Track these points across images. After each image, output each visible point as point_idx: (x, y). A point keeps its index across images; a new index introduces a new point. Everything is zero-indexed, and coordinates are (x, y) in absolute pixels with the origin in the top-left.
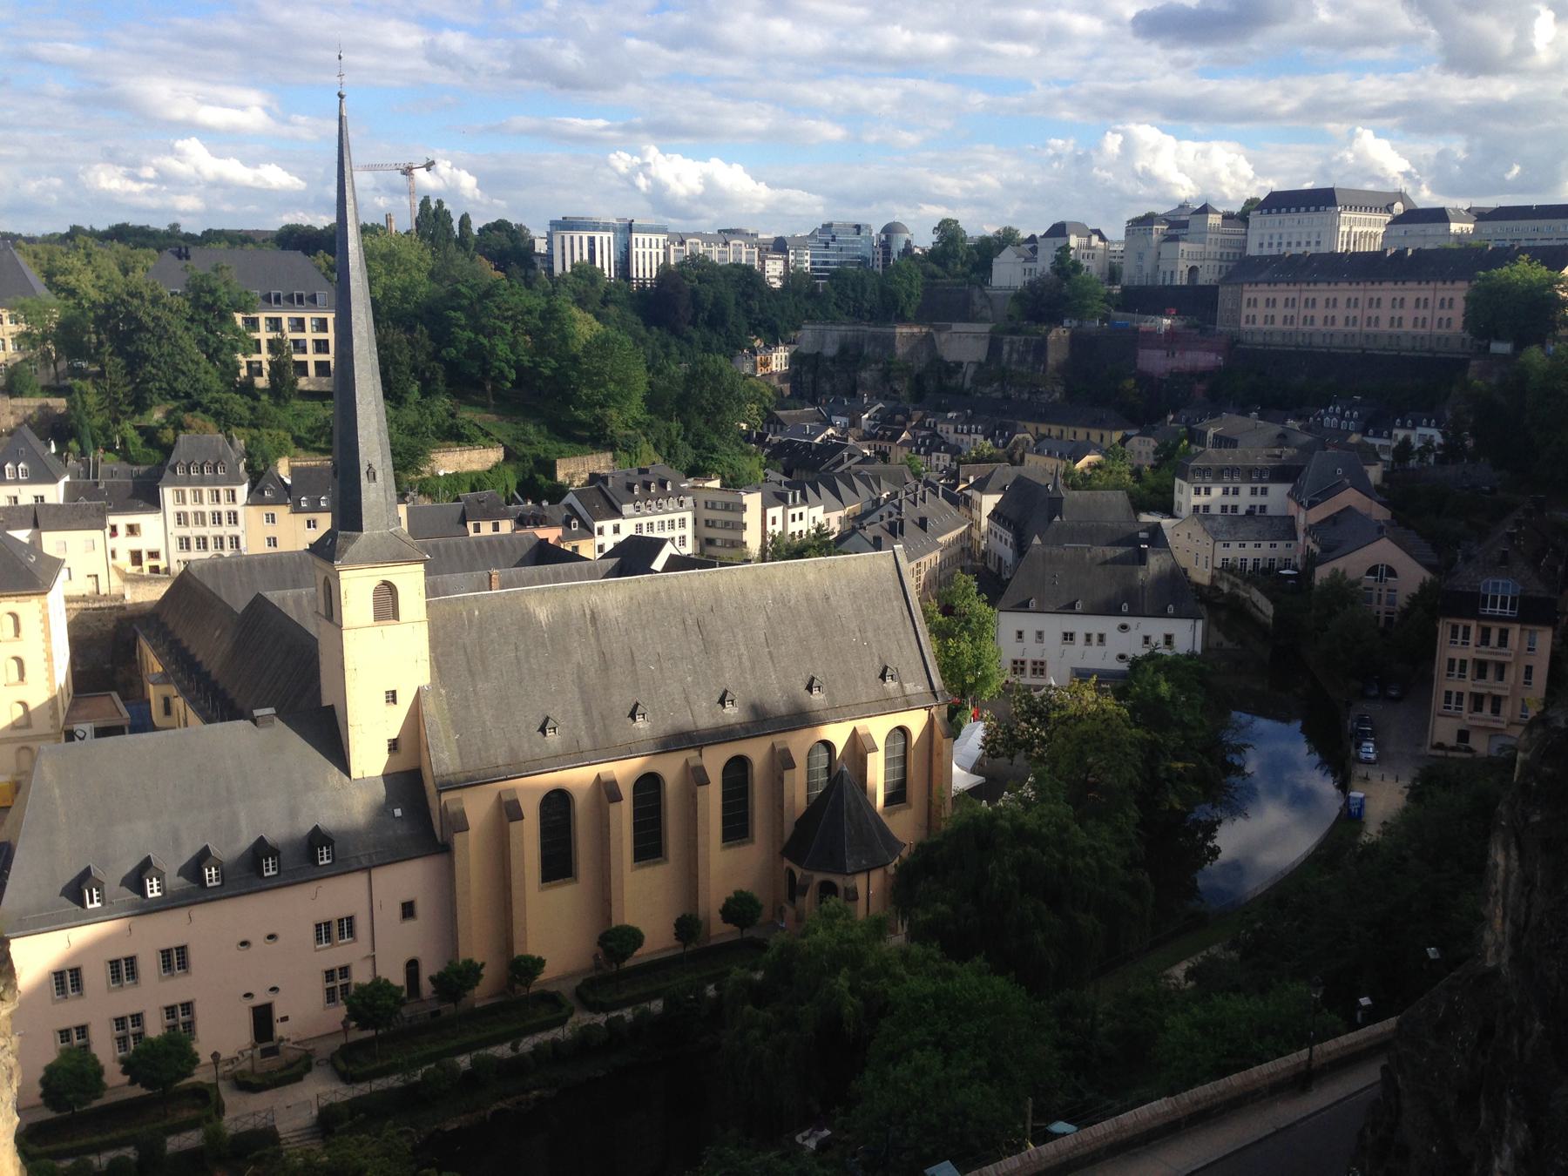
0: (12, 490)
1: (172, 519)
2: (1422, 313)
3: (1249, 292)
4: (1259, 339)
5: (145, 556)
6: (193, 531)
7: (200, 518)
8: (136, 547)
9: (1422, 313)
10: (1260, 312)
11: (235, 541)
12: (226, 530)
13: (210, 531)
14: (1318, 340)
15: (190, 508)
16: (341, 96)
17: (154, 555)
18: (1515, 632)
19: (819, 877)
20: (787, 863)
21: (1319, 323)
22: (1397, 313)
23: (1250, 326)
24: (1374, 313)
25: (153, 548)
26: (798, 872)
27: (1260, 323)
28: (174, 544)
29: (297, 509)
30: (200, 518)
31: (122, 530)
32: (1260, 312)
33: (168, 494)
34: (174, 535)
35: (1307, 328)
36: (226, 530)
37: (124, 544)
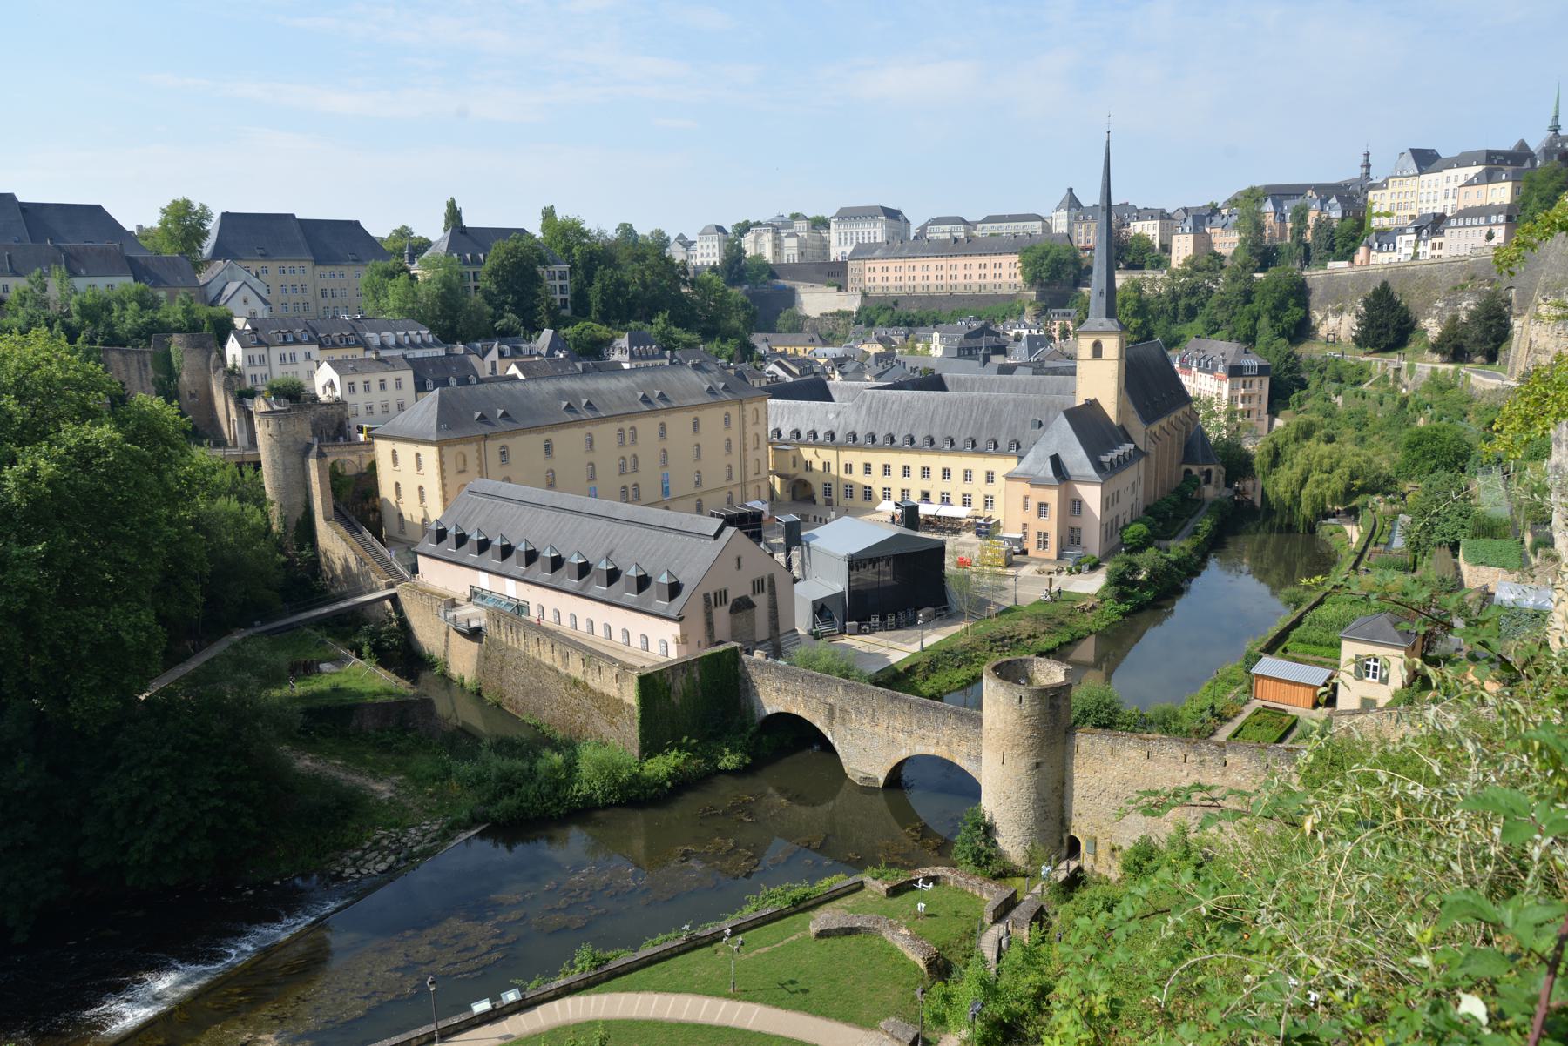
2: (983, 271)
3: (869, 264)
4: (879, 290)
9: (983, 271)
10: (879, 275)
14: (919, 290)
18: (1256, 381)
19: (1205, 468)
20: (1185, 467)
21: (919, 280)
22: (968, 272)
23: (872, 284)
24: (953, 273)
26: (1195, 470)
27: (878, 282)
32: (879, 275)
35: (911, 283)
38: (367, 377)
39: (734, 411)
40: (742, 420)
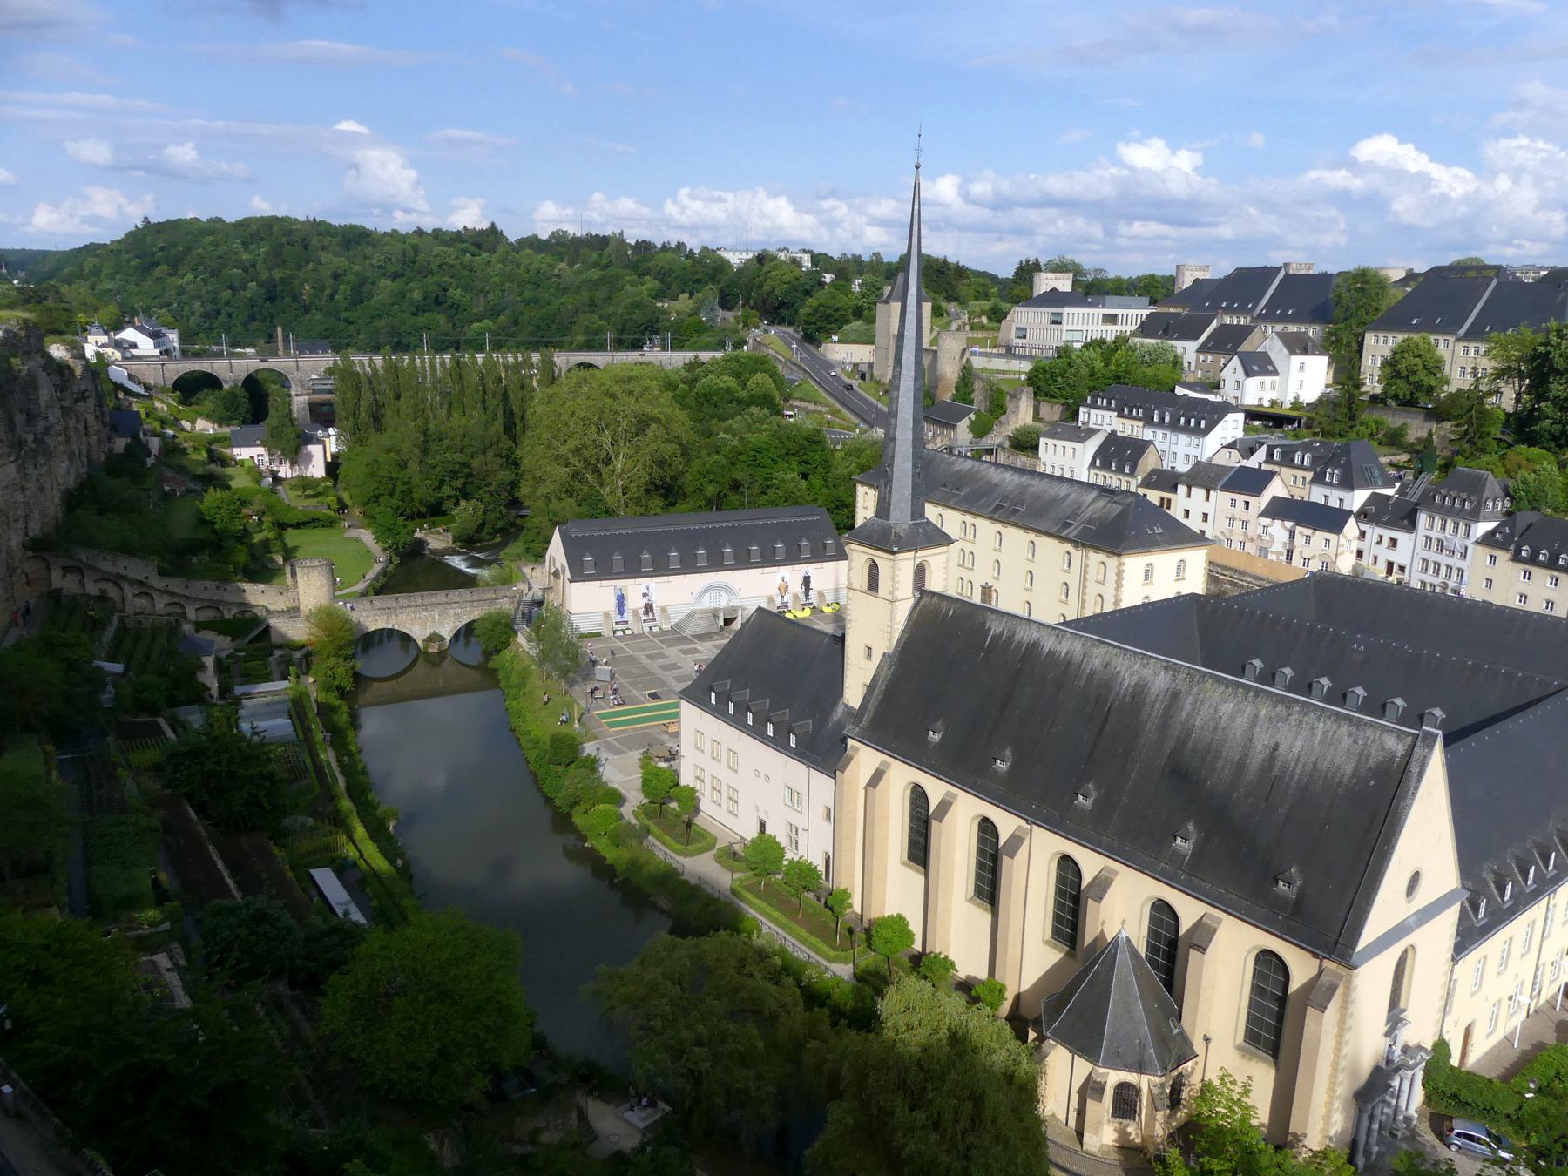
0: (1327, 491)
1: (1421, 541)
5: (1395, 568)
6: (1433, 556)
7: (1441, 546)
8: (1391, 560)
11: (1461, 571)
12: (1456, 562)
13: (1444, 559)
15: (1435, 534)
16: (917, 167)
17: (1402, 569)
25: (1403, 563)
28: (1418, 565)
29: (1517, 558)
30: (1441, 546)
31: (1386, 542)
33: (1423, 518)
34: (1420, 555)
36: (1456, 562)
37: (1385, 554)
38: (1055, 442)
39: (1077, 554)
40: (1085, 568)
